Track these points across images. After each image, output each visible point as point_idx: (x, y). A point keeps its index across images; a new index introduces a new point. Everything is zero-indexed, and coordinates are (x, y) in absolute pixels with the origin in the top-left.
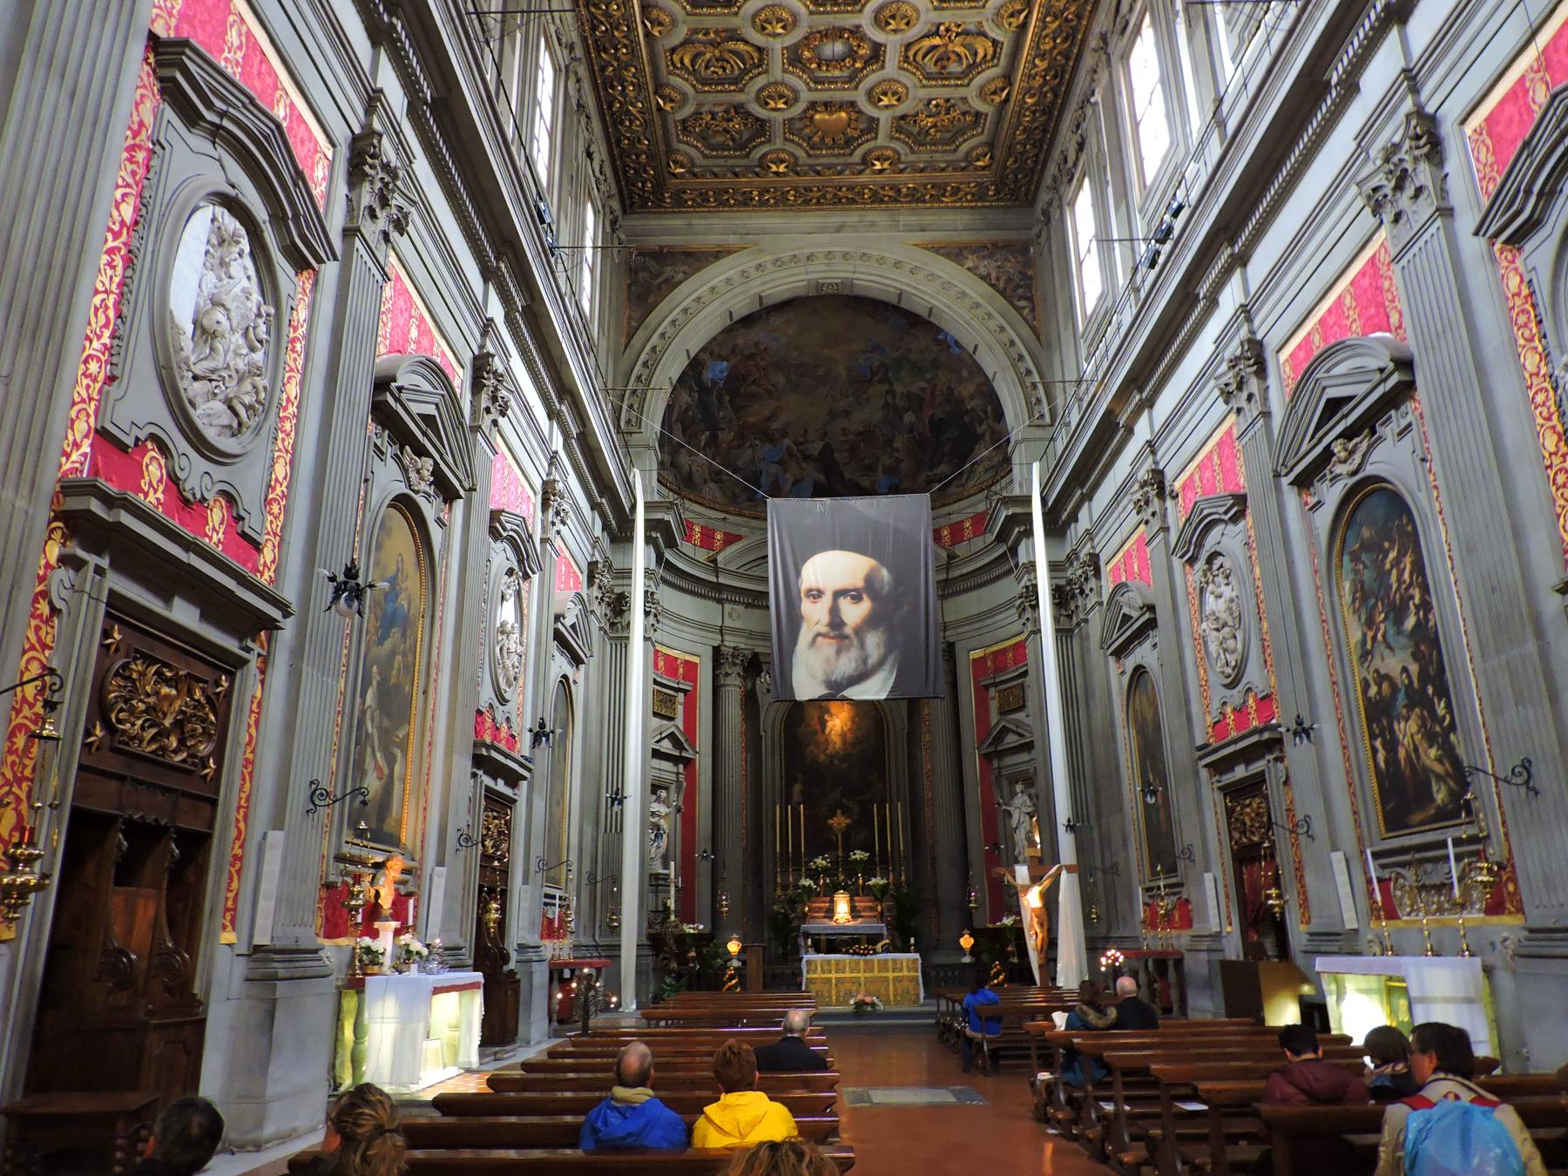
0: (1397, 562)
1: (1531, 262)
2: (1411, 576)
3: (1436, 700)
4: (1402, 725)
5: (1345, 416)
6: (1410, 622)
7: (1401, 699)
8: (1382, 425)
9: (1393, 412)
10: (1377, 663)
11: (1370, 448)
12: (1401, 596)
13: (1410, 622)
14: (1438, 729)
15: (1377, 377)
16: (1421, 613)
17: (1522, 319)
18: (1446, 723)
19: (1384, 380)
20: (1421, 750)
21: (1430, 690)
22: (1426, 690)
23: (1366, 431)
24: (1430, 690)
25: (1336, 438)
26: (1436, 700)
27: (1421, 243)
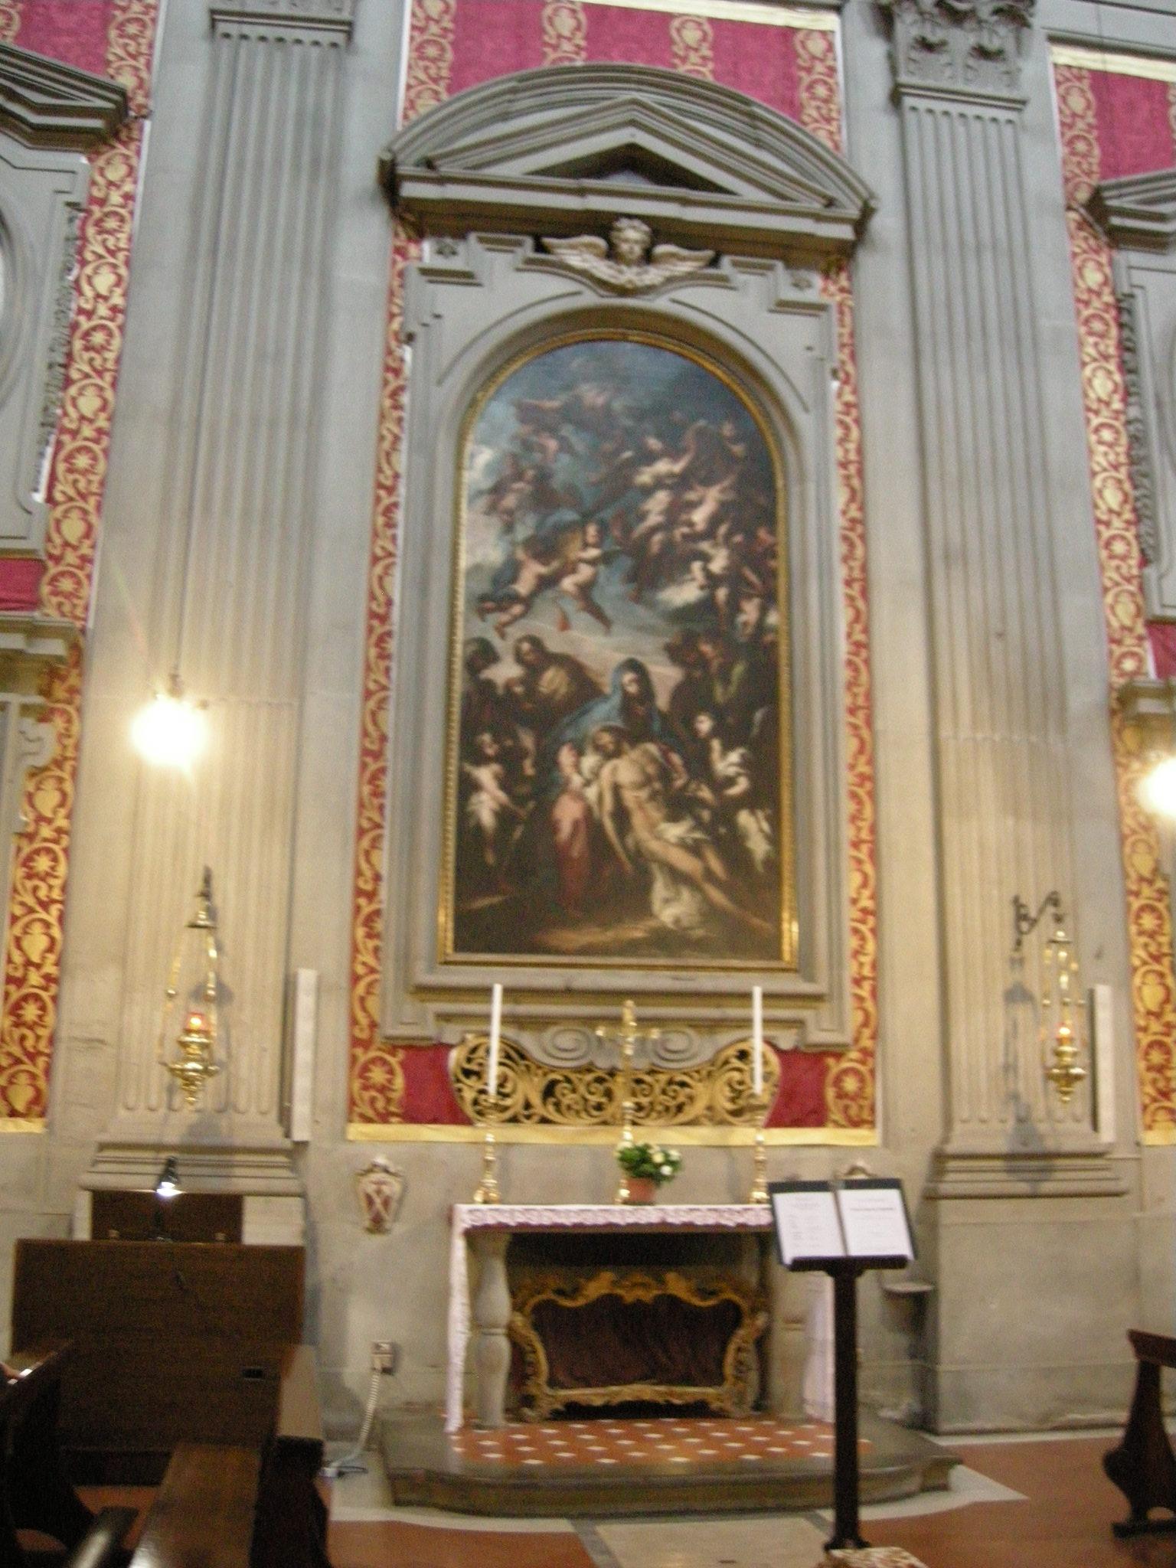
0: (680, 483)
1: (1138, 277)
2: (714, 521)
3: (716, 745)
4: (589, 761)
5: (685, 202)
6: (685, 593)
7: (603, 714)
8: (735, 264)
9: (779, 265)
10: (543, 625)
11: (691, 278)
12: (668, 545)
13: (685, 593)
14: (706, 793)
15: (817, 206)
16: (722, 594)
17: (1097, 326)
18: (735, 791)
19: (818, 218)
20: (638, 820)
21: (704, 724)
22: (689, 722)
23: (709, 253)
24: (704, 724)
25: (644, 219)
26: (716, 745)
27: (971, 111)
